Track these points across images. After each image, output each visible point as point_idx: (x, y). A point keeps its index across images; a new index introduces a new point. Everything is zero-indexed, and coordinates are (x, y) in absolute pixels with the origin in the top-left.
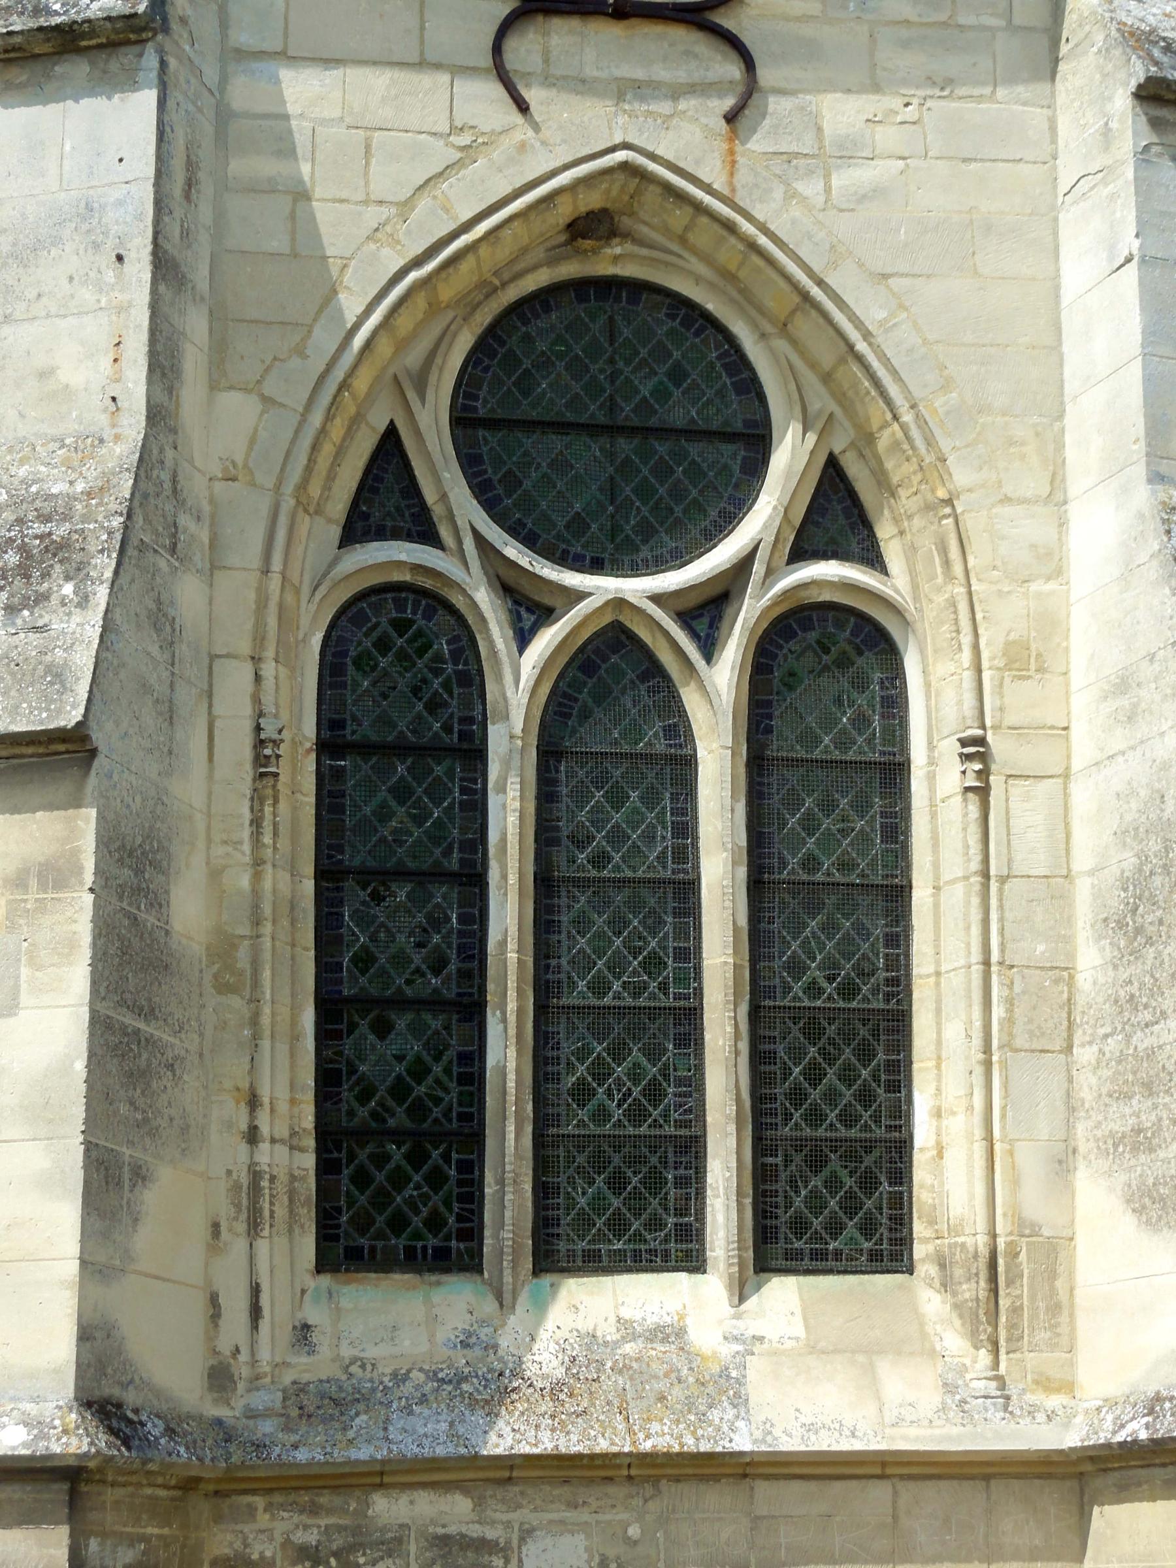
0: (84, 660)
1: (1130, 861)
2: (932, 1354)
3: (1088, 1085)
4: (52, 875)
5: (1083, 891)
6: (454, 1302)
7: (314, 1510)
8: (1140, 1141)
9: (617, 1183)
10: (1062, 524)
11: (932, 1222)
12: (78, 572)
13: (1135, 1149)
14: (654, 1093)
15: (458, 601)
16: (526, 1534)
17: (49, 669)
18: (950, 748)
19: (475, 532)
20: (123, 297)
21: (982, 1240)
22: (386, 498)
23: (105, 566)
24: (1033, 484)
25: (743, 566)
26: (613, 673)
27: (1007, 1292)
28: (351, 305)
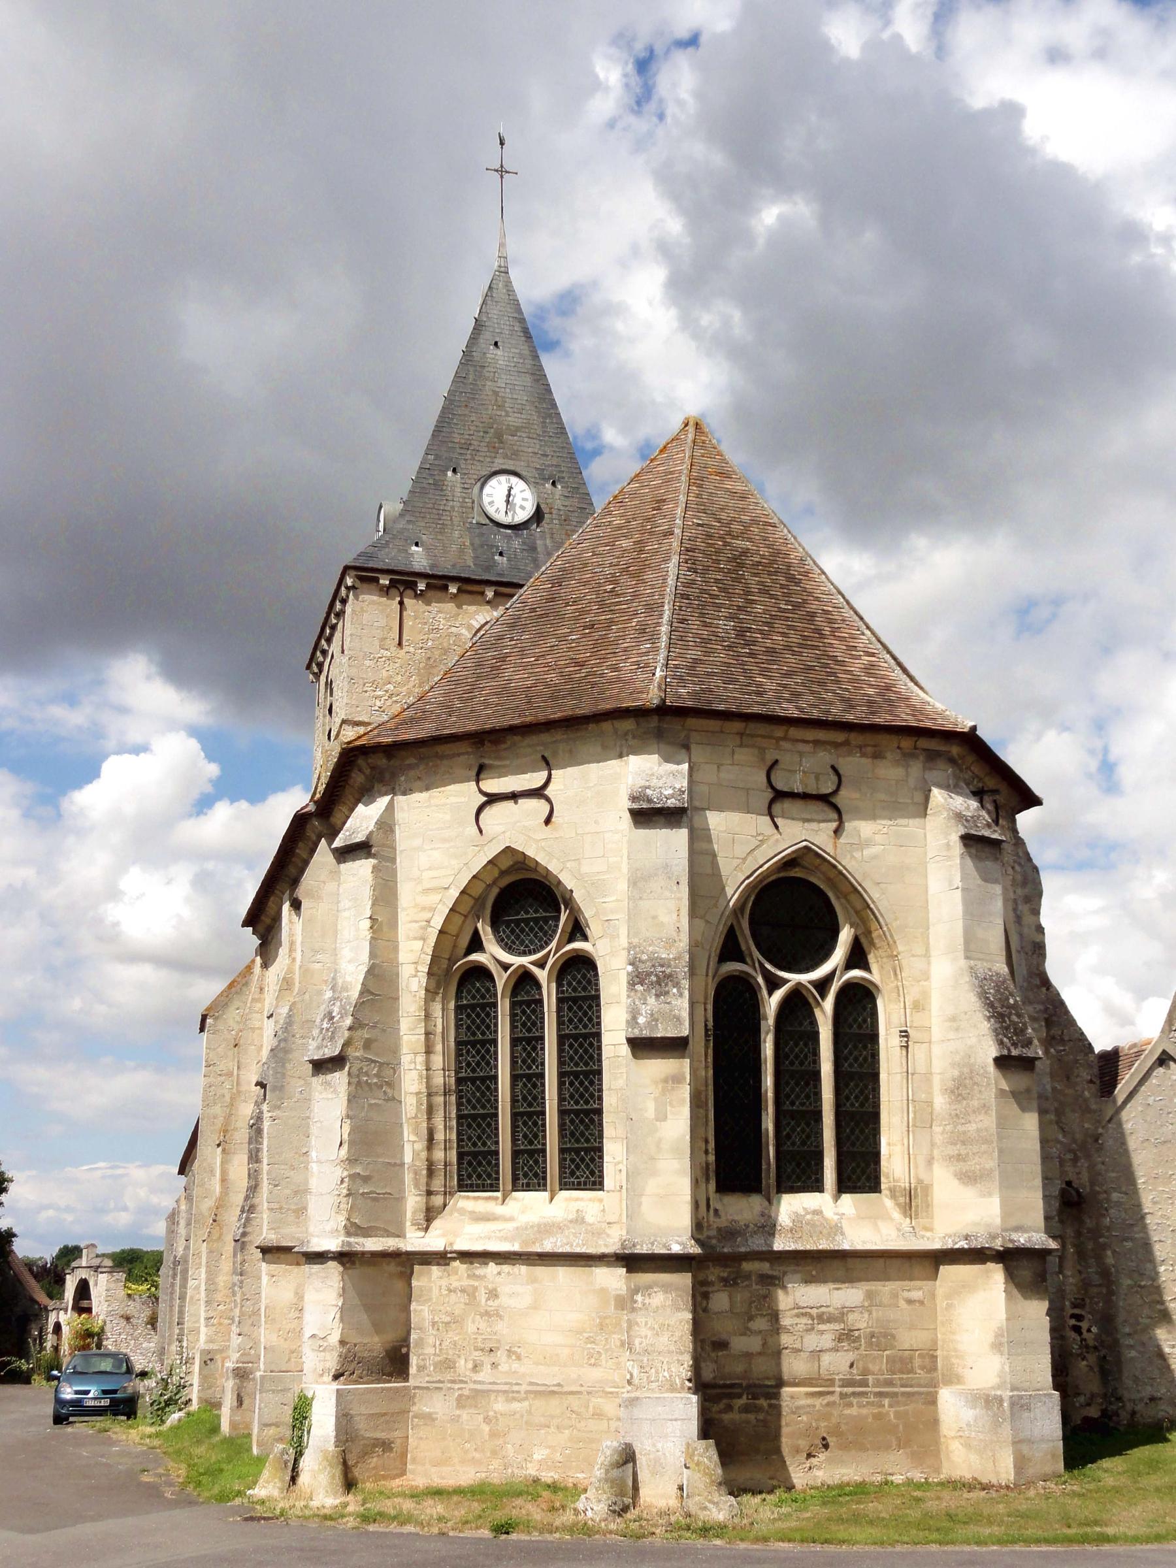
0: (685, 1014)
1: (956, 1073)
2: (892, 1219)
3: (938, 1139)
4: (677, 1079)
5: (936, 1081)
6: (755, 1202)
7: (726, 1266)
8: (960, 1158)
9: (798, 1165)
10: (929, 963)
11: (888, 1178)
12: (677, 985)
13: (958, 1160)
14: (808, 1137)
15: (752, 981)
16: (785, 1273)
17: (675, 1016)
18: (895, 1032)
19: (760, 962)
20: (678, 895)
21: (907, 1185)
22: (730, 949)
23: (685, 984)
24: (920, 950)
25: (833, 973)
26: (798, 1006)
27: (912, 1201)
28: (729, 891)
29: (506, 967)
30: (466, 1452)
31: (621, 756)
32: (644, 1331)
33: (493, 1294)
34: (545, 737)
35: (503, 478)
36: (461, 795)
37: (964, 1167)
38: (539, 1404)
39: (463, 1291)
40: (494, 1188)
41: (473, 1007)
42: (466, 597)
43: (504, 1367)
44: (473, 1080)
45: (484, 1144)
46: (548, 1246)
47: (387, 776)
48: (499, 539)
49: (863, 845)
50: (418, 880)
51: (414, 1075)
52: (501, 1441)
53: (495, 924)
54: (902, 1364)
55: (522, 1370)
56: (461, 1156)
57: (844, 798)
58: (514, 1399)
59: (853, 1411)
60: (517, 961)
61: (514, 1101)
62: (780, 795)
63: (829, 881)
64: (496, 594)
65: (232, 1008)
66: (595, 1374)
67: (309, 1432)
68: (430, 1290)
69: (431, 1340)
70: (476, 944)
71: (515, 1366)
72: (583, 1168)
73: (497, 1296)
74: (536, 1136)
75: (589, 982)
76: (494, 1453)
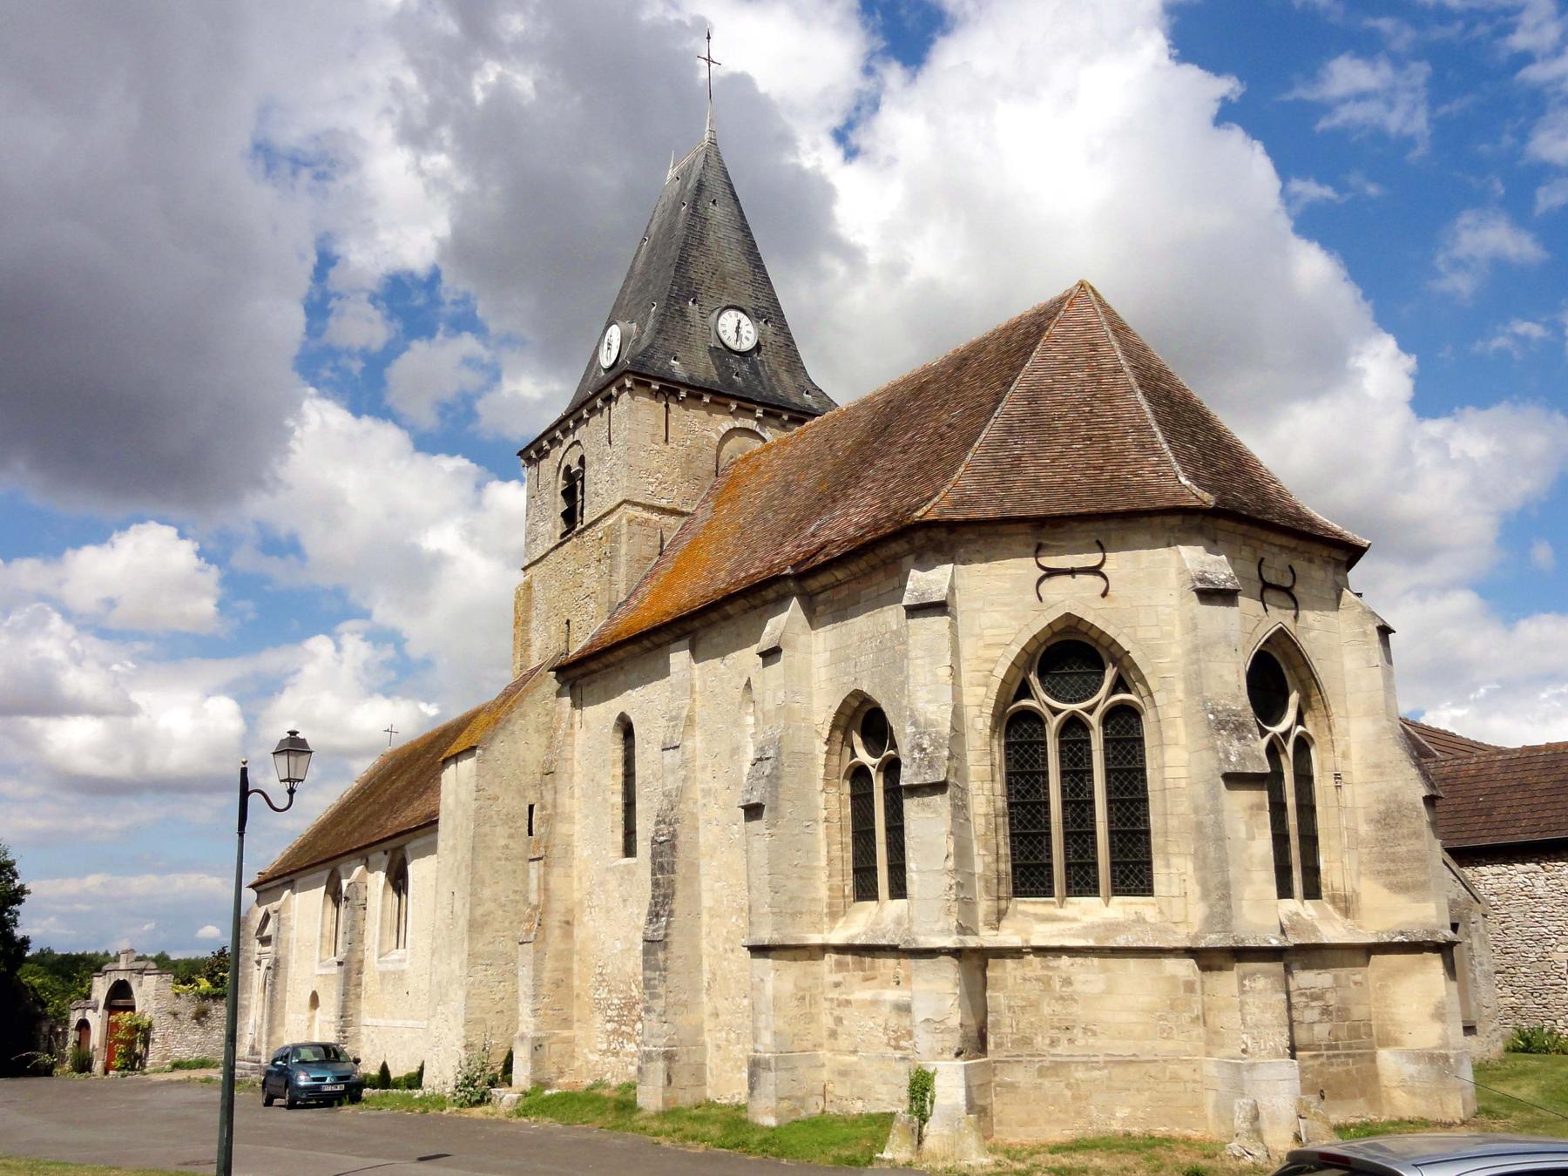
1: (1382, 808)
4: (1260, 807)
8: (1388, 872)
12: (1250, 731)
29: (1056, 712)
30: (1050, 1114)
31: (1169, 545)
33: (1067, 982)
34: (1100, 525)
35: (733, 312)
36: (1023, 568)
37: (1395, 880)
38: (1118, 1071)
39: (1037, 979)
40: (1049, 892)
41: (1021, 745)
43: (1080, 1042)
44: (1024, 805)
45: (1036, 858)
46: (1121, 941)
48: (732, 361)
49: (1309, 629)
50: (980, 637)
51: (982, 799)
52: (1084, 1103)
53: (1041, 676)
54: (1354, 1032)
55: (1099, 1043)
56: (1014, 867)
57: (1298, 590)
58: (1094, 1068)
59: (1333, 1069)
60: (1070, 707)
61: (1065, 822)
62: (1266, 586)
63: (1286, 656)
64: (739, 407)
65: (498, 740)
66: (1169, 1045)
67: (932, 1102)
69: (1008, 1021)
70: (1025, 691)
71: (1091, 1041)
72: (1134, 876)
74: (1086, 852)
75: (1132, 727)
76: (1078, 1113)
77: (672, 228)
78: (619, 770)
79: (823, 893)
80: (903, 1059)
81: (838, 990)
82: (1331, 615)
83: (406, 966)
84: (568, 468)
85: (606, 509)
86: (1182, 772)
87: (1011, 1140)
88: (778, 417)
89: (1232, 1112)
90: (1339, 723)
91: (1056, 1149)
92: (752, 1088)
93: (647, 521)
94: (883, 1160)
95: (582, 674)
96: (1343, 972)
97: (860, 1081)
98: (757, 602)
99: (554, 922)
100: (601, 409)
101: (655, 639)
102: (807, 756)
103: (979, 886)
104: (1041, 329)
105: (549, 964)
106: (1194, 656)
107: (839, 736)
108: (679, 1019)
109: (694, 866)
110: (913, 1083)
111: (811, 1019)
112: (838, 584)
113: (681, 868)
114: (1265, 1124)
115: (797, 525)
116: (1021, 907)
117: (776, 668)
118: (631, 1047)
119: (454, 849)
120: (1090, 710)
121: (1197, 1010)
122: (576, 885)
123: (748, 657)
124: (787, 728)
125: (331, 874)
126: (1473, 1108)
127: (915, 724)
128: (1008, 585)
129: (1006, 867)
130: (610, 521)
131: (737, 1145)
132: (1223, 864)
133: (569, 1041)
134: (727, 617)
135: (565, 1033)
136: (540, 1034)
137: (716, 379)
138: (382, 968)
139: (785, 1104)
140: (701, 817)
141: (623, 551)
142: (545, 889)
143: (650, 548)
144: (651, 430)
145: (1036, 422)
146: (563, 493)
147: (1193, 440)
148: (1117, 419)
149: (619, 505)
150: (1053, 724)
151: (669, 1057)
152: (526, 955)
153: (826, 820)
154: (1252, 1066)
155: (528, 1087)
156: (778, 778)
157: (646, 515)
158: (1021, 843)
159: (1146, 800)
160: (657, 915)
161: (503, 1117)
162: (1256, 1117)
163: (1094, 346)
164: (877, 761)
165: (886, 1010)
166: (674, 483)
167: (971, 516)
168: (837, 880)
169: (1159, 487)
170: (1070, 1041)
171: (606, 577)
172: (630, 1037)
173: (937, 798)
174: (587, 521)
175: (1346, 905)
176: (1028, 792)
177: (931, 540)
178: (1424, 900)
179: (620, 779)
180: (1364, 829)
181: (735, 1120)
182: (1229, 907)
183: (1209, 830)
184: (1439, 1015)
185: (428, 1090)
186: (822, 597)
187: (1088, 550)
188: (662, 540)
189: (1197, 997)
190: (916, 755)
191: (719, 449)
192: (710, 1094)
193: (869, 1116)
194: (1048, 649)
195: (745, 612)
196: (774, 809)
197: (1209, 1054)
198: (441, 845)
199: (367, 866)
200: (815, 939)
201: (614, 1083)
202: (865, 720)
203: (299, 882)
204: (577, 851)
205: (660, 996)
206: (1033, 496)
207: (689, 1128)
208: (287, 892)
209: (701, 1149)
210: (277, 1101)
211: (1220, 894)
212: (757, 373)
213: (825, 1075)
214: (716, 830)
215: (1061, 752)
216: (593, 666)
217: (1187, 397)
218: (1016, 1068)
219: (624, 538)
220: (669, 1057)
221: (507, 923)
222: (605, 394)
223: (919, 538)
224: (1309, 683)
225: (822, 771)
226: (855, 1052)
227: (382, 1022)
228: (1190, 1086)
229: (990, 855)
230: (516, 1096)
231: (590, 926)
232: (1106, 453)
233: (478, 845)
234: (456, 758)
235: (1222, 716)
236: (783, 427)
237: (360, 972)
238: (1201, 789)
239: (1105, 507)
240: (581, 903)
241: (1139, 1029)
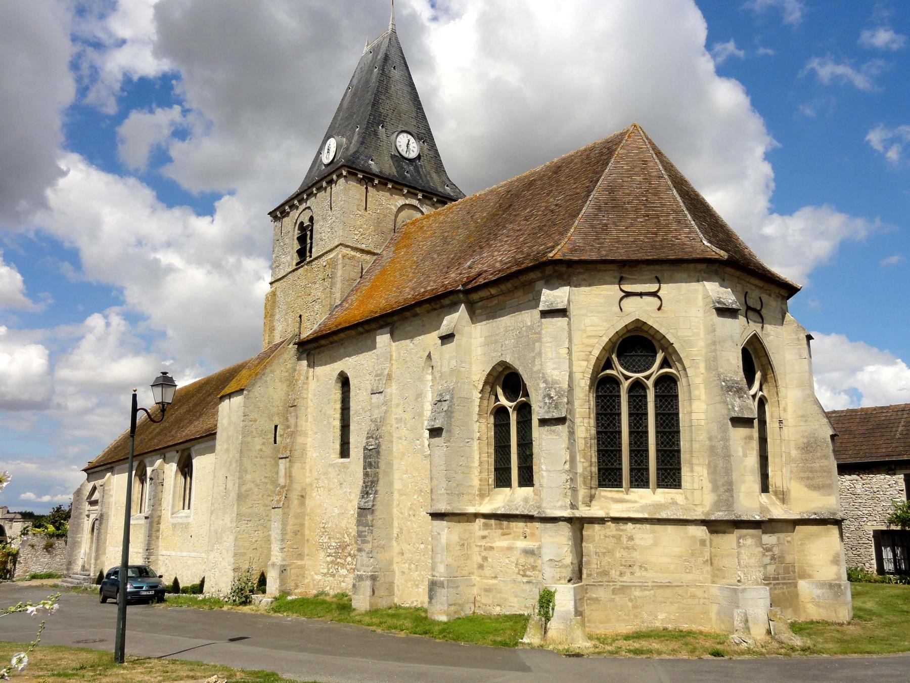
1: (805, 441)
8: (808, 478)
29: (627, 378)
30: (619, 616)
31: (698, 281)
32: (744, 557)
33: (631, 538)
34: (658, 267)
35: (405, 135)
36: (612, 291)
37: (812, 482)
38: (659, 592)
39: (613, 537)
40: (619, 485)
41: (605, 397)
42: (394, 190)
43: (638, 574)
44: (606, 433)
46: (663, 515)
47: (565, 277)
49: (768, 335)
50: (585, 331)
52: (639, 610)
53: (618, 356)
55: (649, 575)
56: (599, 470)
57: (763, 312)
58: (645, 590)
62: (749, 308)
63: (756, 351)
64: (408, 192)
66: (690, 577)
67: (553, 609)
68: (594, 536)
69: (595, 561)
70: (608, 365)
71: (644, 573)
72: (670, 476)
73: (633, 539)
74: (642, 462)
76: (636, 616)
77: (368, 81)
78: (338, 406)
79: (476, 482)
80: (528, 582)
81: (484, 541)
82: (779, 328)
83: (190, 520)
84: (302, 223)
85: (328, 249)
86: (702, 416)
87: (598, 632)
88: (431, 199)
89: (732, 618)
90: (782, 391)
91: (627, 638)
92: (431, 598)
93: (353, 257)
94: (524, 644)
95: (314, 348)
96: (782, 535)
97: (499, 596)
98: (438, 306)
99: (294, 496)
100: (326, 188)
101: (366, 327)
102: (468, 400)
103: (580, 480)
104: (611, 152)
105: (291, 521)
106: (713, 348)
107: (488, 388)
108: (379, 556)
109: (390, 464)
110: (542, 597)
111: (467, 557)
112: (492, 296)
113: (382, 465)
114: (751, 624)
115: (456, 261)
116: (603, 494)
117: (450, 347)
118: (343, 572)
119: (228, 450)
120: (648, 378)
121: (707, 556)
122: (308, 474)
123: (431, 339)
124: (457, 383)
125: (139, 465)
126: (851, 615)
127: (545, 382)
128: (602, 301)
129: (595, 469)
130: (332, 255)
131: (426, 633)
132: (728, 471)
133: (302, 567)
134: (416, 315)
135: (299, 563)
136: (285, 563)
137: (396, 174)
138: (175, 521)
139: (453, 608)
140: (394, 435)
141: (339, 273)
142: (289, 476)
143: (355, 273)
144: (357, 202)
145: (613, 204)
146: (298, 238)
147: (705, 221)
148: (663, 205)
149: (337, 247)
150: (625, 385)
151: (374, 578)
152: (277, 515)
153: (479, 439)
154: (744, 590)
155: (278, 595)
156: (452, 412)
157: (353, 253)
158: (604, 455)
159: (678, 432)
160: (367, 493)
161: (265, 613)
162: (747, 621)
163: (645, 162)
164: (514, 404)
165: (517, 553)
166: (369, 235)
167: (583, 258)
168: (485, 475)
169: (692, 247)
170: (632, 573)
171: (328, 290)
172: (343, 566)
173: (560, 427)
174: (314, 255)
175: (783, 497)
176: (608, 425)
177: (556, 271)
178: (829, 495)
179: (339, 411)
180: (794, 453)
181: (419, 619)
182: (732, 496)
183: (719, 451)
184: (836, 561)
185: (208, 595)
186: (480, 304)
187: (650, 281)
188: (362, 269)
189: (707, 549)
190: (547, 400)
191: (396, 217)
192: (397, 600)
193: (506, 616)
194: (624, 340)
195: (428, 312)
196: (449, 431)
197: (713, 582)
198: (218, 447)
199: (164, 459)
200: (471, 510)
201: (332, 593)
202: (507, 379)
203: (117, 468)
204: (309, 454)
205: (368, 542)
206: (618, 248)
207: (390, 621)
208: (109, 474)
209: (403, 634)
210: (109, 600)
211: (725, 488)
212: (418, 172)
213: (475, 591)
214: (405, 443)
215: (629, 402)
216: (323, 342)
217: (697, 195)
218: (600, 589)
219: (340, 267)
220: (374, 578)
221: (260, 496)
222: (328, 179)
223: (549, 270)
224: (767, 367)
225: (477, 409)
226: (496, 577)
227: (173, 553)
228: (702, 601)
229: (587, 462)
230: (270, 600)
231: (316, 499)
232: (657, 224)
233: (244, 448)
234: (230, 395)
235: (730, 384)
236: (433, 205)
237: (159, 523)
238: (714, 427)
239: (662, 256)
240: (311, 484)
241: (672, 567)
